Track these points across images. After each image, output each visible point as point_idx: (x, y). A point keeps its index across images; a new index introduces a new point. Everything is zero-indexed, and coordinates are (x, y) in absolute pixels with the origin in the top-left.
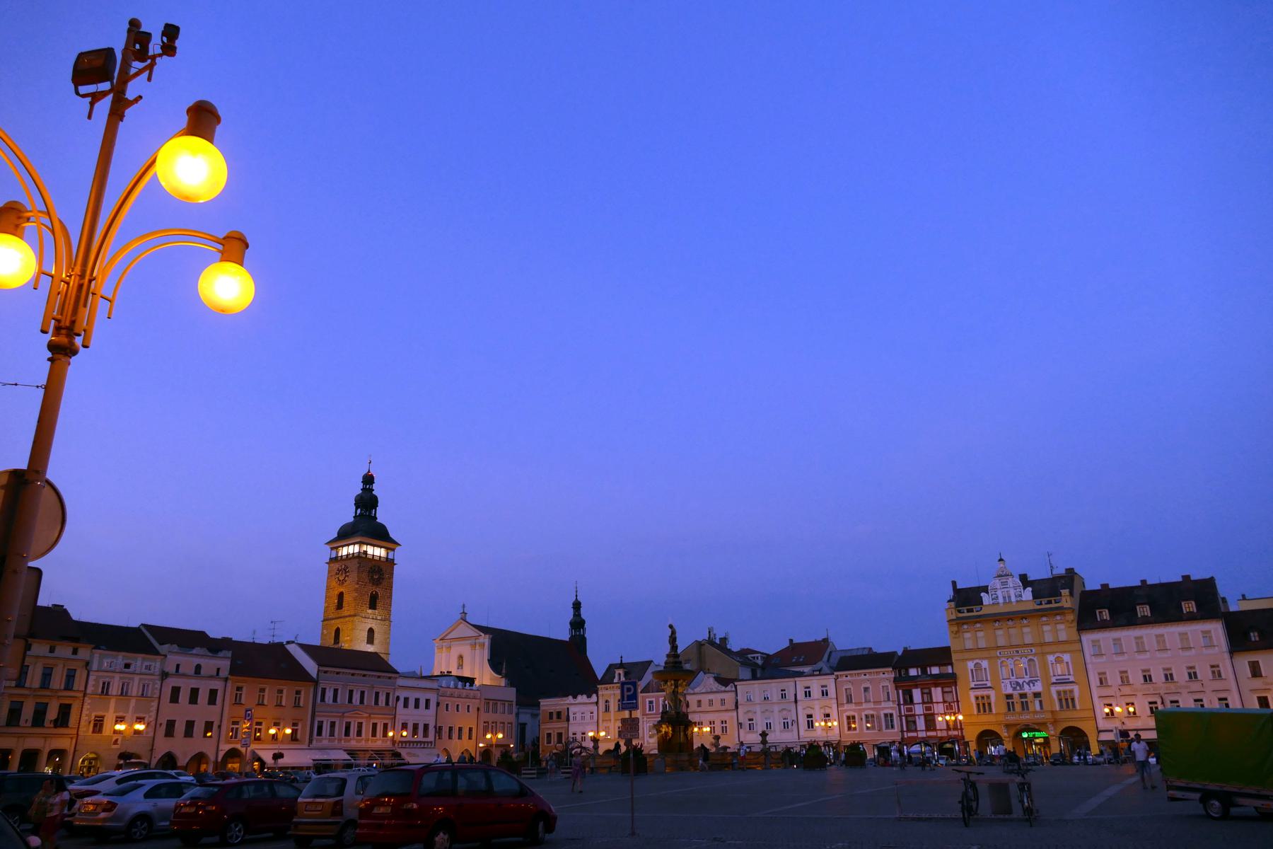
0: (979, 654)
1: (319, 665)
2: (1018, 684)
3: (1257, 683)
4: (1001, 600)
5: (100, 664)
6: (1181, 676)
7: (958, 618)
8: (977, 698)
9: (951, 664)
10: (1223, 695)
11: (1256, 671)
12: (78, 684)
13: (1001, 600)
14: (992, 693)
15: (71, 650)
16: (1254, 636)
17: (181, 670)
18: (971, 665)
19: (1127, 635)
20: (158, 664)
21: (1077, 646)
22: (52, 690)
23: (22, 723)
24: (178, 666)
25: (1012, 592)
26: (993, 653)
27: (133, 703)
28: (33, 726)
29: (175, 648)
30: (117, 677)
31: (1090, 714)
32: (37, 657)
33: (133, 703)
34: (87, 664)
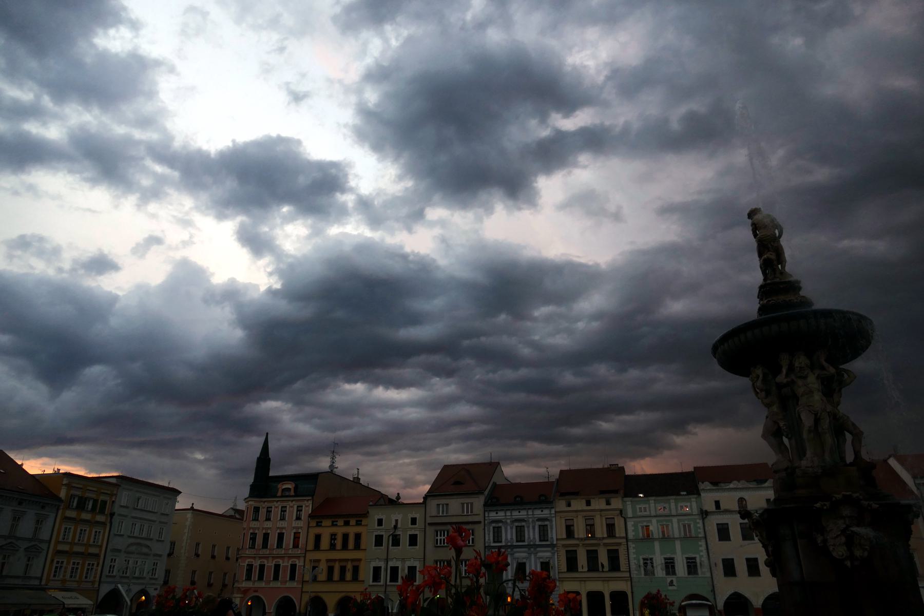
1: (915, 477)
5: (634, 511)
12: (619, 531)
15: (603, 502)
17: (723, 507)
20: (694, 505)
22: (597, 539)
23: (580, 569)
24: (717, 504)
27: (678, 544)
28: (589, 570)
29: (706, 485)
30: (654, 520)
32: (576, 511)
33: (678, 544)
34: (621, 511)
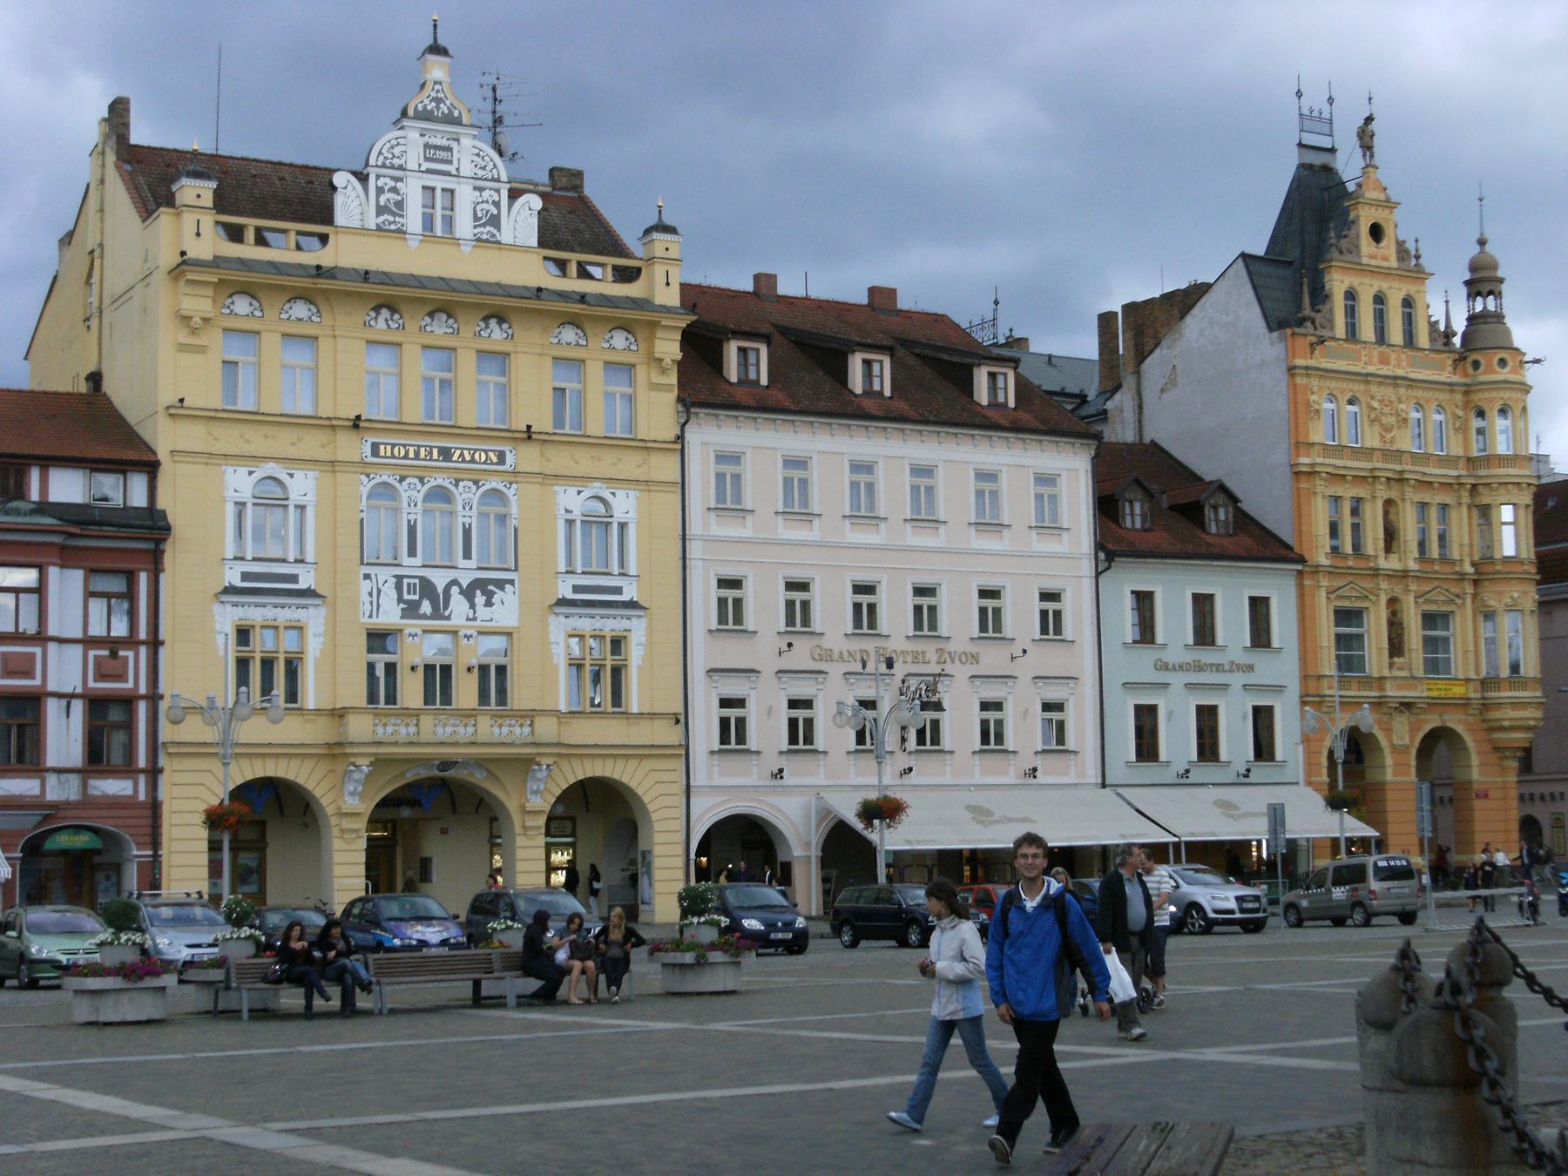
0: (284, 441)
2: (427, 588)
3: (1141, 665)
4: (413, 220)
6: (958, 614)
7: (218, 262)
8: (243, 634)
9: (151, 467)
10: (1053, 694)
11: (1146, 632)
13: (413, 220)
14: (314, 618)
16: (1134, 515)
18: (240, 482)
19: (829, 448)
21: (665, 467)
25: (466, 197)
26: (355, 448)
31: (672, 735)
